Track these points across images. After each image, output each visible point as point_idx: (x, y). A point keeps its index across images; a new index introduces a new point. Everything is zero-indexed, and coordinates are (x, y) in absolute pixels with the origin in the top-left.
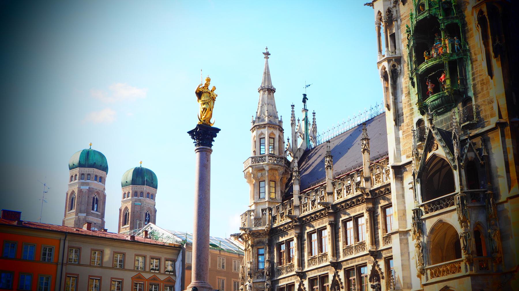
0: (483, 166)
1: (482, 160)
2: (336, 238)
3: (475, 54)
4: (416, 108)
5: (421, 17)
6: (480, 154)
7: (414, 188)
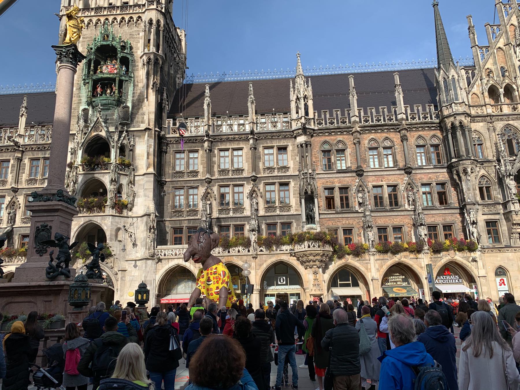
3: (137, 82)
4: (84, 99)
5: (105, 43)
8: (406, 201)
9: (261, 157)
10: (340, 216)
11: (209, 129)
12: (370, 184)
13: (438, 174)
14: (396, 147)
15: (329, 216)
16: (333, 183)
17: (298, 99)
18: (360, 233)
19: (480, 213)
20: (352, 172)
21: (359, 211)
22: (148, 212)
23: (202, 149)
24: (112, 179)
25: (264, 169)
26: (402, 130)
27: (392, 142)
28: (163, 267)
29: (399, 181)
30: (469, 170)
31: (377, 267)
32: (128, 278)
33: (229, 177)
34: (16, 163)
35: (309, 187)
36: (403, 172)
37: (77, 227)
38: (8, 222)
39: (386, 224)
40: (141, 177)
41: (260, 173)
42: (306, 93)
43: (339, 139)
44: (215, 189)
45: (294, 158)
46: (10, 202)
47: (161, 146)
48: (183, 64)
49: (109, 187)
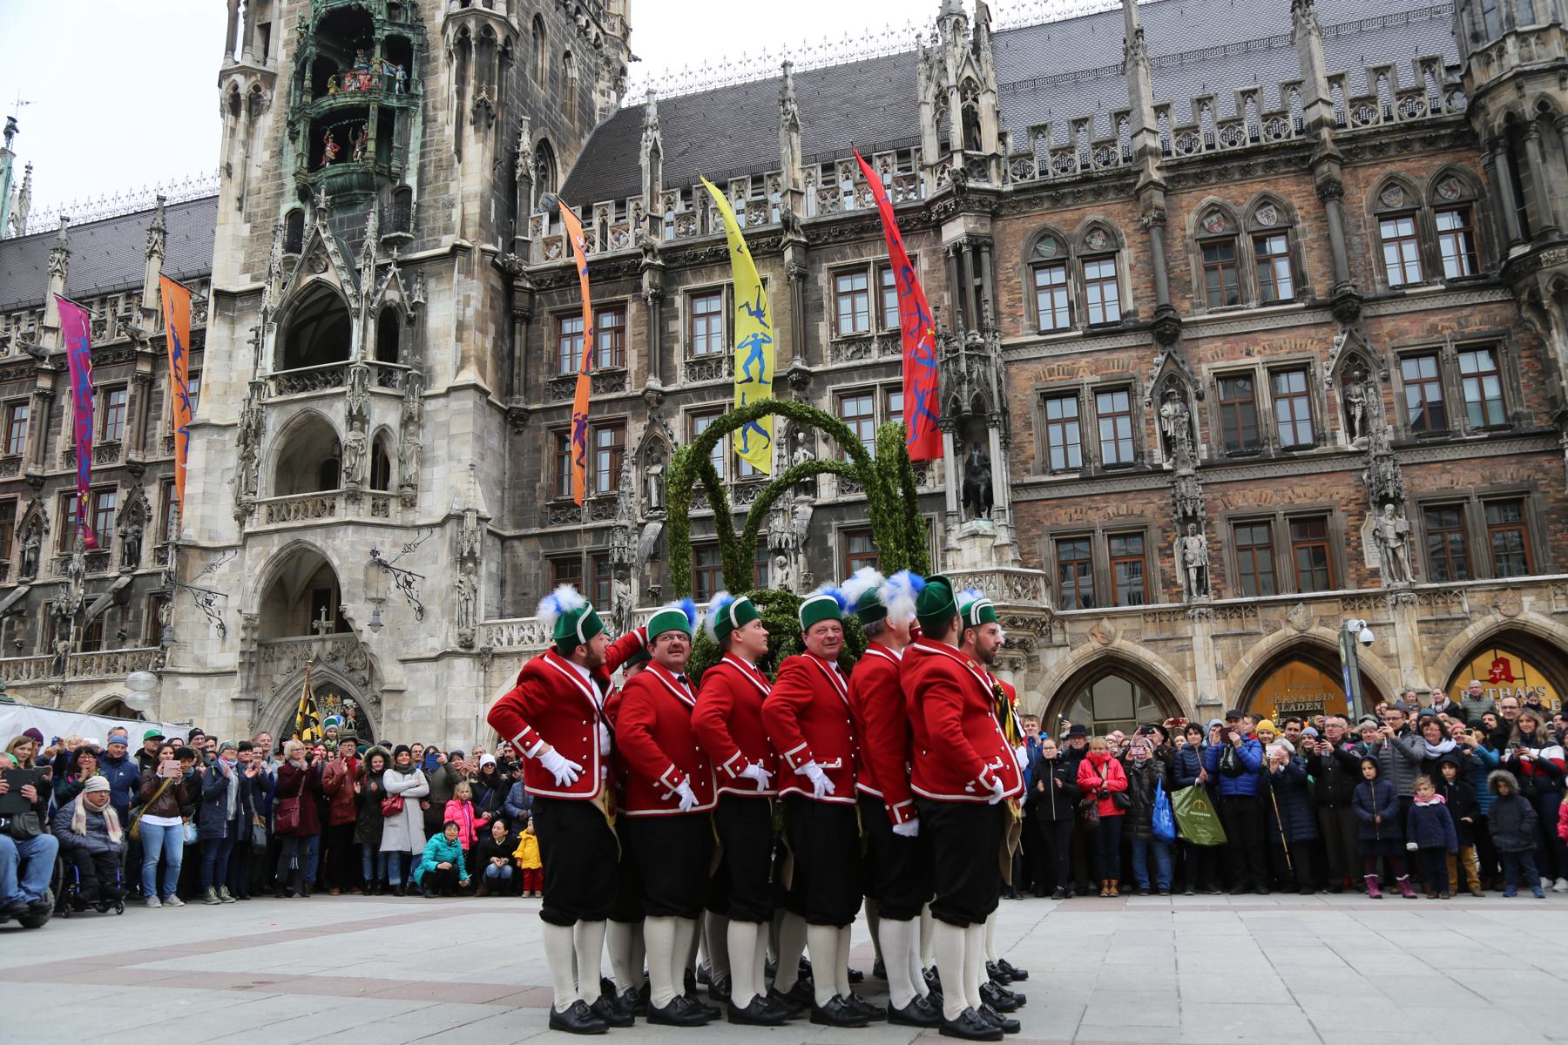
0: (411, 321)
2: (48, 427)
3: (435, 108)
4: (291, 184)
6: (410, 297)
7: (258, 344)
9: (825, 303)
10: (1097, 488)
11: (654, 230)
12: (1204, 367)
13: (1465, 312)
14: (1299, 227)
15: (1056, 493)
16: (1072, 373)
17: (942, 97)
18: (1171, 546)
20: (1138, 329)
21: (1166, 466)
22: (457, 507)
23: (638, 298)
24: (350, 411)
25: (836, 346)
26: (1320, 161)
27: (1286, 210)
29: (1314, 349)
31: (1219, 661)
32: (408, 715)
33: (721, 381)
34: (139, 393)
35: (965, 387)
36: (1326, 316)
37: (263, 562)
38: (123, 561)
39: (1266, 507)
40: (442, 401)
41: (819, 359)
42: (969, 72)
43: (1090, 218)
44: (677, 423)
46: (126, 503)
48: (616, 46)
49: (346, 436)
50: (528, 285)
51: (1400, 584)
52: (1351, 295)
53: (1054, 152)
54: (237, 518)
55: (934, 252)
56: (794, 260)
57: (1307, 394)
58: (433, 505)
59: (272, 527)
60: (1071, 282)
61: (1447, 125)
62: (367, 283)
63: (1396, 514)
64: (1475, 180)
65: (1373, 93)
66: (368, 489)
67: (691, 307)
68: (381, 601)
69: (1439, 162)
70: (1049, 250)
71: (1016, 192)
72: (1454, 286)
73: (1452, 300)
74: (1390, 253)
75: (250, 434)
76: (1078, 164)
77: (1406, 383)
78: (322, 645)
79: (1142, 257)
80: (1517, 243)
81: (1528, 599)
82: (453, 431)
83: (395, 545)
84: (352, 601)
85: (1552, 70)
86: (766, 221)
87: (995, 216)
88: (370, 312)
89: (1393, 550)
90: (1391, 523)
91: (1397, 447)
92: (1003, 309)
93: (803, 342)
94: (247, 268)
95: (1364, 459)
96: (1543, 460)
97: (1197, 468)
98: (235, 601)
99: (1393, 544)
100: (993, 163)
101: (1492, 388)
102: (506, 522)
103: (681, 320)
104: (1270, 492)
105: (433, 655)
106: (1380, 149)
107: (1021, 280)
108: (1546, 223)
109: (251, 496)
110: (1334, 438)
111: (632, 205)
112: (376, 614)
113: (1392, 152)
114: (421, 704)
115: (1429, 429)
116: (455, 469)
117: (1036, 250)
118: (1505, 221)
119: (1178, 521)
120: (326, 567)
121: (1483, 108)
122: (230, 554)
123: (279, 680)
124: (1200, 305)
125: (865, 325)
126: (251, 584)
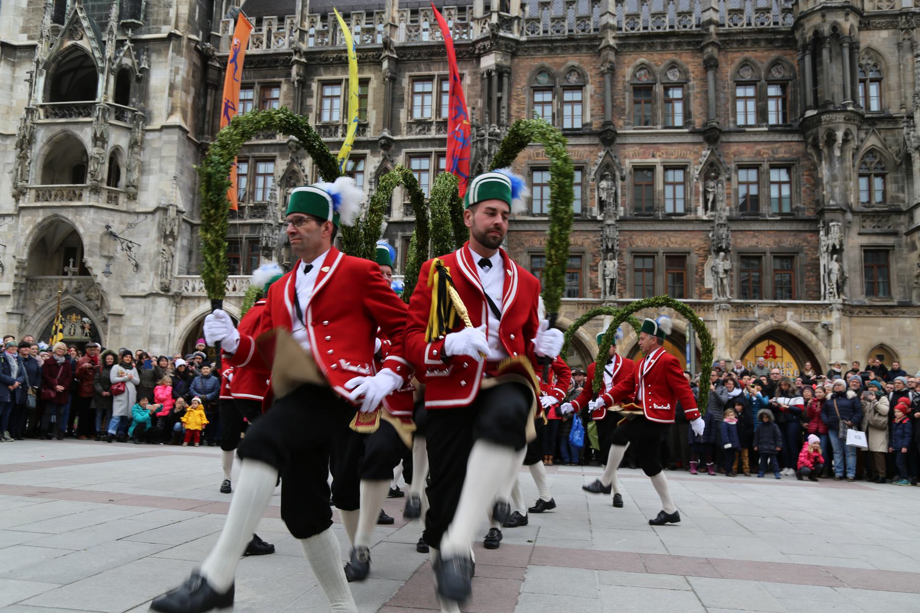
0: (139, 80)
1: (140, 72)
6: (139, 64)
7: (31, 82)
8: (701, 200)
9: (406, 97)
11: (301, 38)
12: (627, 161)
13: (777, 145)
14: (691, 83)
15: (534, 227)
18: (597, 265)
19: (855, 229)
20: (591, 134)
21: (599, 218)
22: (164, 203)
24: (95, 134)
25: (410, 125)
26: (707, 45)
27: (685, 72)
28: (188, 312)
29: (691, 158)
30: (840, 135)
32: (125, 330)
33: (337, 139)
35: (486, 159)
36: (700, 139)
37: (31, 227)
39: (654, 247)
40: (157, 134)
43: (570, 63)
45: (472, 101)
47: (207, 75)
49: (91, 150)
50: (218, 65)
51: (722, 299)
52: (715, 128)
53: (553, 20)
54: (14, 196)
55: (475, 73)
56: (389, 68)
57: (683, 183)
58: (148, 200)
59: (39, 204)
60: (555, 101)
61: (781, 33)
62: (110, 51)
63: (725, 258)
64: (792, 67)
65: (742, 7)
66: (105, 186)
67: (322, 90)
68: (110, 258)
69: (774, 55)
70: (544, 80)
71: (528, 42)
72: (773, 129)
73: (771, 138)
74: (740, 105)
75: (25, 143)
76: (566, 29)
77: (740, 183)
78: (69, 283)
79: (598, 91)
80: (810, 108)
81: (790, 313)
82: (164, 154)
83: (122, 223)
84: (91, 256)
85: (842, 8)
86: (373, 41)
87: (514, 55)
88: (111, 71)
89: (721, 279)
90: (722, 263)
91: (730, 220)
92: (513, 113)
93: (391, 121)
94: (25, 30)
95: (711, 225)
96: (808, 235)
97: (617, 221)
98: (11, 250)
99: (721, 276)
100: (516, 22)
101: (786, 191)
102: (195, 215)
103: (315, 99)
104: (657, 239)
105: (143, 294)
106: (742, 42)
107: (525, 96)
108: (827, 98)
109: (24, 183)
110: (696, 211)
111: (288, 21)
112: (108, 266)
113: (749, 45)
114: (134, 324)
115: (749, 210)
116: (164, 179)
117: (536, 79)
118: (805, 94)
119: (603, 251)
120: (74, 233)
121: (802, 25)
122: (8, 220)
123: (40, 302)
124: (629, 124)
125: (429, 114)
126: (22, 240)
